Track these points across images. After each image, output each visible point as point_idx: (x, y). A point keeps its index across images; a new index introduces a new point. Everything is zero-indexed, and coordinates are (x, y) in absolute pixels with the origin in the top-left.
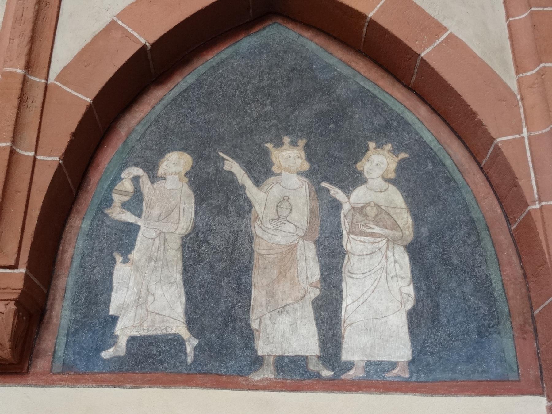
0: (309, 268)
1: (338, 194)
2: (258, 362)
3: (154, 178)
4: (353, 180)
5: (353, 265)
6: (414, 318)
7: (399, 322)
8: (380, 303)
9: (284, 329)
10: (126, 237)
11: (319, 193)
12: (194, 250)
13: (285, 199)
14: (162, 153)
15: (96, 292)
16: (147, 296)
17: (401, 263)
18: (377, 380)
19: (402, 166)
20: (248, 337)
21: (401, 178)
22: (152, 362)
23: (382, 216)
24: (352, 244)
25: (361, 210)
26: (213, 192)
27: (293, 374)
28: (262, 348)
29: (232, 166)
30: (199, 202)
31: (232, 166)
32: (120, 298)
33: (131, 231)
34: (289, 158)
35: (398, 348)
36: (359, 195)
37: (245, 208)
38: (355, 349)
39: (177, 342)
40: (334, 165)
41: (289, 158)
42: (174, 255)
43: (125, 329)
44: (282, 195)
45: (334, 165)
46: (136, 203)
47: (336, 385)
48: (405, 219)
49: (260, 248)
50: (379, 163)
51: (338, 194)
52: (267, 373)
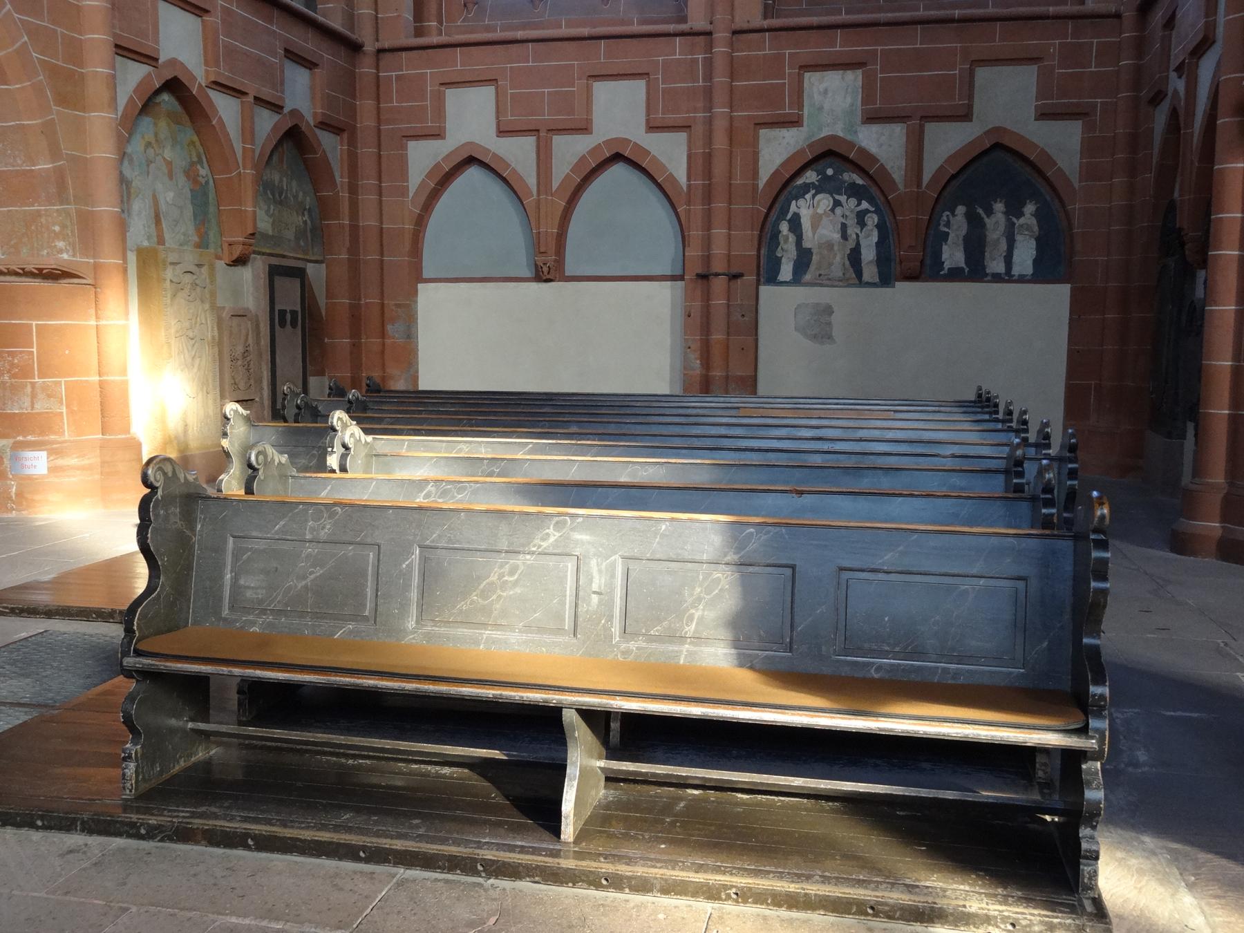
0: (1004, 246)
1: (1014, 220)
2: (987, 275)
3: (954, 215)
4: (1020, 214)
5: (1017, 244)
6: (1035, 261)
7: (1030, 263)
8: (1025, 255)
9: (996, 265)
10: (946, 236)
11: (1008, 220)
13: (997, 222)
14: (955, 207)
15: (937, 254)
16: (953, 255)
18: (1022, 279)
19: (1037, 210)
20: (984, 267)
21: (1037, 214)
22: (955, 275)
23: (1029, 228)
24: (1018, 238)
25: (1021, 226)
26: (975, 223)
27: (997, 278)
28: (988, 271)
29: (980, 211)
30: (969, 223)
31: (980, 211)
32: (945, 256)
33: (948, 234)
34: (999, 207)
35: (1028, 270)
36: (1022, 220)
37: (983, 226)
38: (1016, 271)
39: (962, 269)
40: (1014, 210)
41: (999, 207)
42: (961, 241)
43: (947, 265)
44: (996, 222)
45: (1014, 210)
46: (948, 224)
48: (1036, 229)
49: (988, 239)
50: (1030, 208)
51: (1014, 220)
52: (989, 278)
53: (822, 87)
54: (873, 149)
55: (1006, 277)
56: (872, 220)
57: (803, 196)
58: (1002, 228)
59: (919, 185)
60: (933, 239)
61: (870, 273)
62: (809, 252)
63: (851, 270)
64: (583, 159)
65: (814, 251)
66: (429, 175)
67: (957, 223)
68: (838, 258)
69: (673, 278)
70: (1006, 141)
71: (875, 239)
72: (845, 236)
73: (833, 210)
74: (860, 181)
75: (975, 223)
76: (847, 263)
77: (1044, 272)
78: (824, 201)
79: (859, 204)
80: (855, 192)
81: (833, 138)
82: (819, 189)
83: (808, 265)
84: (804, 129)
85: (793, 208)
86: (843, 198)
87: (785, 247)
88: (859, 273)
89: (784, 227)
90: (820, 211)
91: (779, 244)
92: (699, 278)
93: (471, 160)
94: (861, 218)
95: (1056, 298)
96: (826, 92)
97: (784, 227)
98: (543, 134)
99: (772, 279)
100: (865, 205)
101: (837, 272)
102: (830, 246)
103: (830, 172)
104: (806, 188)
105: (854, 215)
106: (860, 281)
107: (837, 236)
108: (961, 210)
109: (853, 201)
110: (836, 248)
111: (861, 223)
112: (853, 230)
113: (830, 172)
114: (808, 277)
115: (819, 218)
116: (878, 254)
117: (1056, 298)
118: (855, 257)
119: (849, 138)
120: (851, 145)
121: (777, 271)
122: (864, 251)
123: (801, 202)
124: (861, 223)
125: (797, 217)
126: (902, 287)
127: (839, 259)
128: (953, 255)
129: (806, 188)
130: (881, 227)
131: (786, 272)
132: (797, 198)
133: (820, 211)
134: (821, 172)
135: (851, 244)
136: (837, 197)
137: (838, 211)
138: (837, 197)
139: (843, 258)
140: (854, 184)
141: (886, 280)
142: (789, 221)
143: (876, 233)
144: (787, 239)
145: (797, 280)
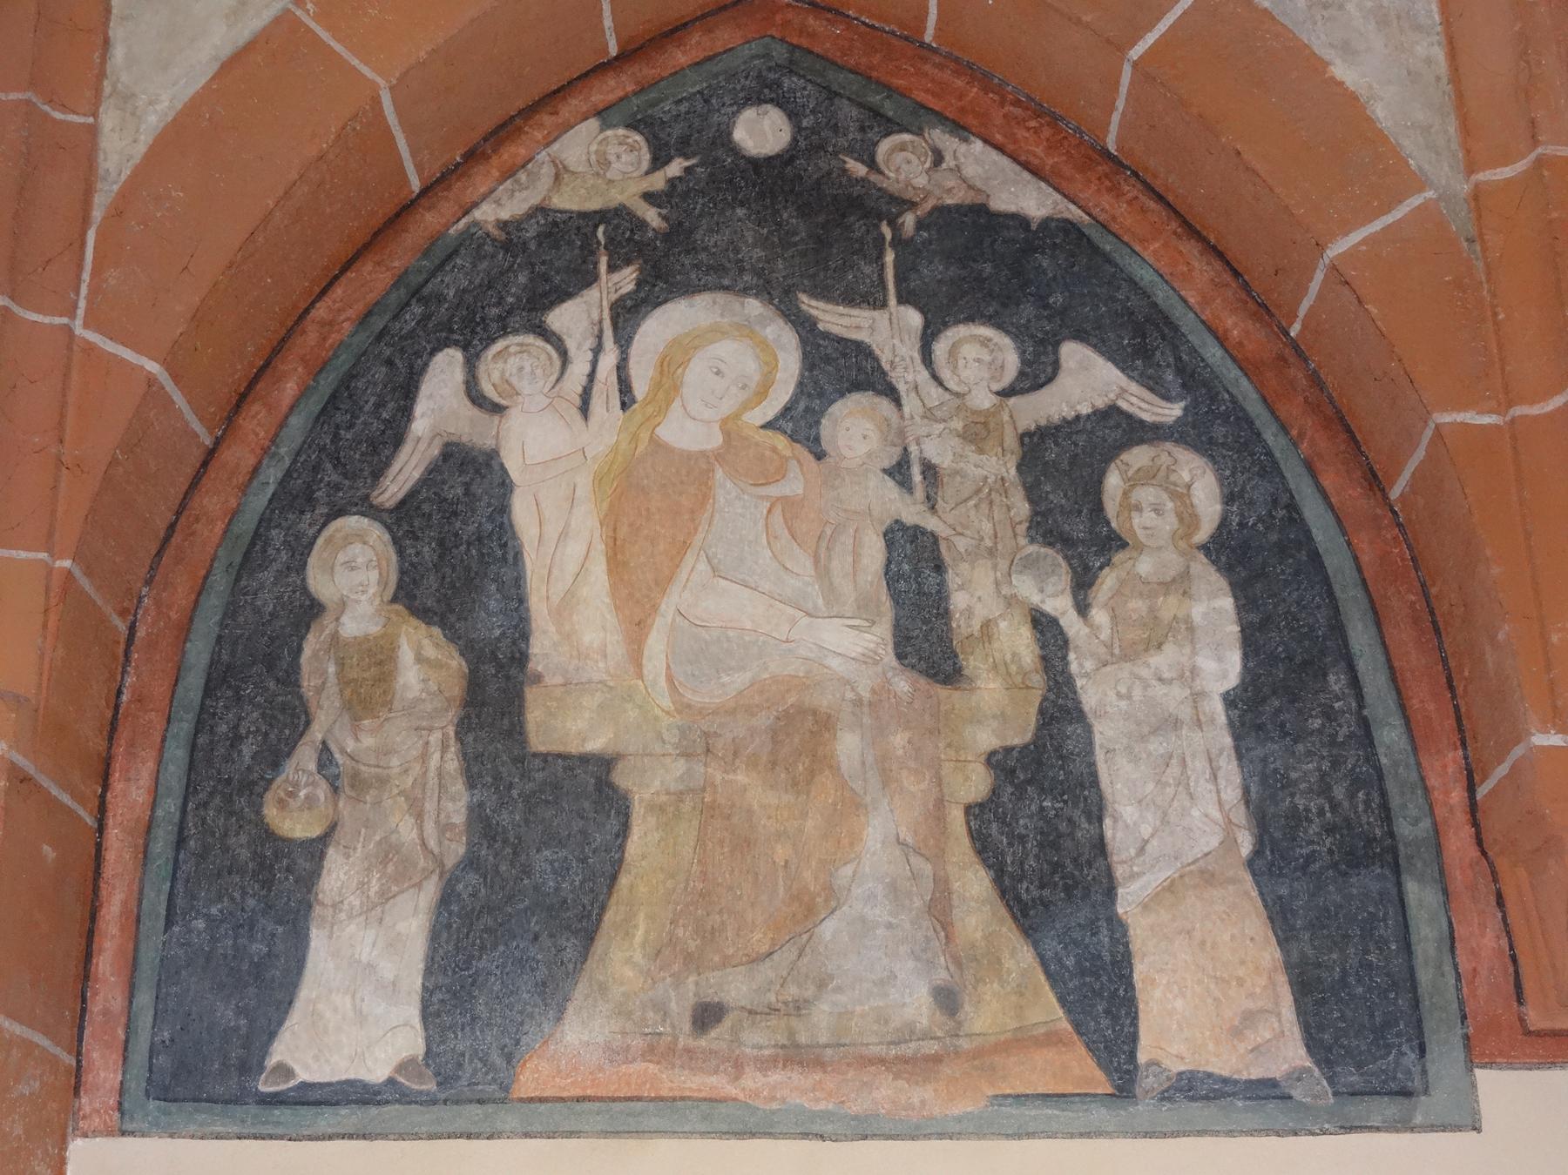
56: (1170, 498)
57: (531, 313)
62: (590, 794)
63: (1020, 958)
65: (645, 786)
71: (1224, 668)
72: (927, 640)
73: (801, 422)
74: (1031, 200)
76: (974, 883)
78: (722, 356)
79: (1037, 372)
82: (667, 261)
85: (439, 403)
86: (889, 331)
87: (357, 744)
88: (1100, 995)
89: (352, 571)
91: (291, 718)
94: (1066, 492)
97: (352, 571)
100: (1088, 379)
105: (1001, 465)
107: (849, 644)
109: (980, 355)
110: (848, 746)
118: (1041, 839)
121: (270, 984)
123: (514, 362)
125: (471, 477)
130: (1262, 556)
131: (358, 997)
132: (473, 330)
133: (687, 430)
135: (995, 710)
136: (835, 319)
137: (854, 426)
138: (835, 319)
139: (931, 846)
142: (403, 520)
143: (1214, 607)
145: (462, 1073)
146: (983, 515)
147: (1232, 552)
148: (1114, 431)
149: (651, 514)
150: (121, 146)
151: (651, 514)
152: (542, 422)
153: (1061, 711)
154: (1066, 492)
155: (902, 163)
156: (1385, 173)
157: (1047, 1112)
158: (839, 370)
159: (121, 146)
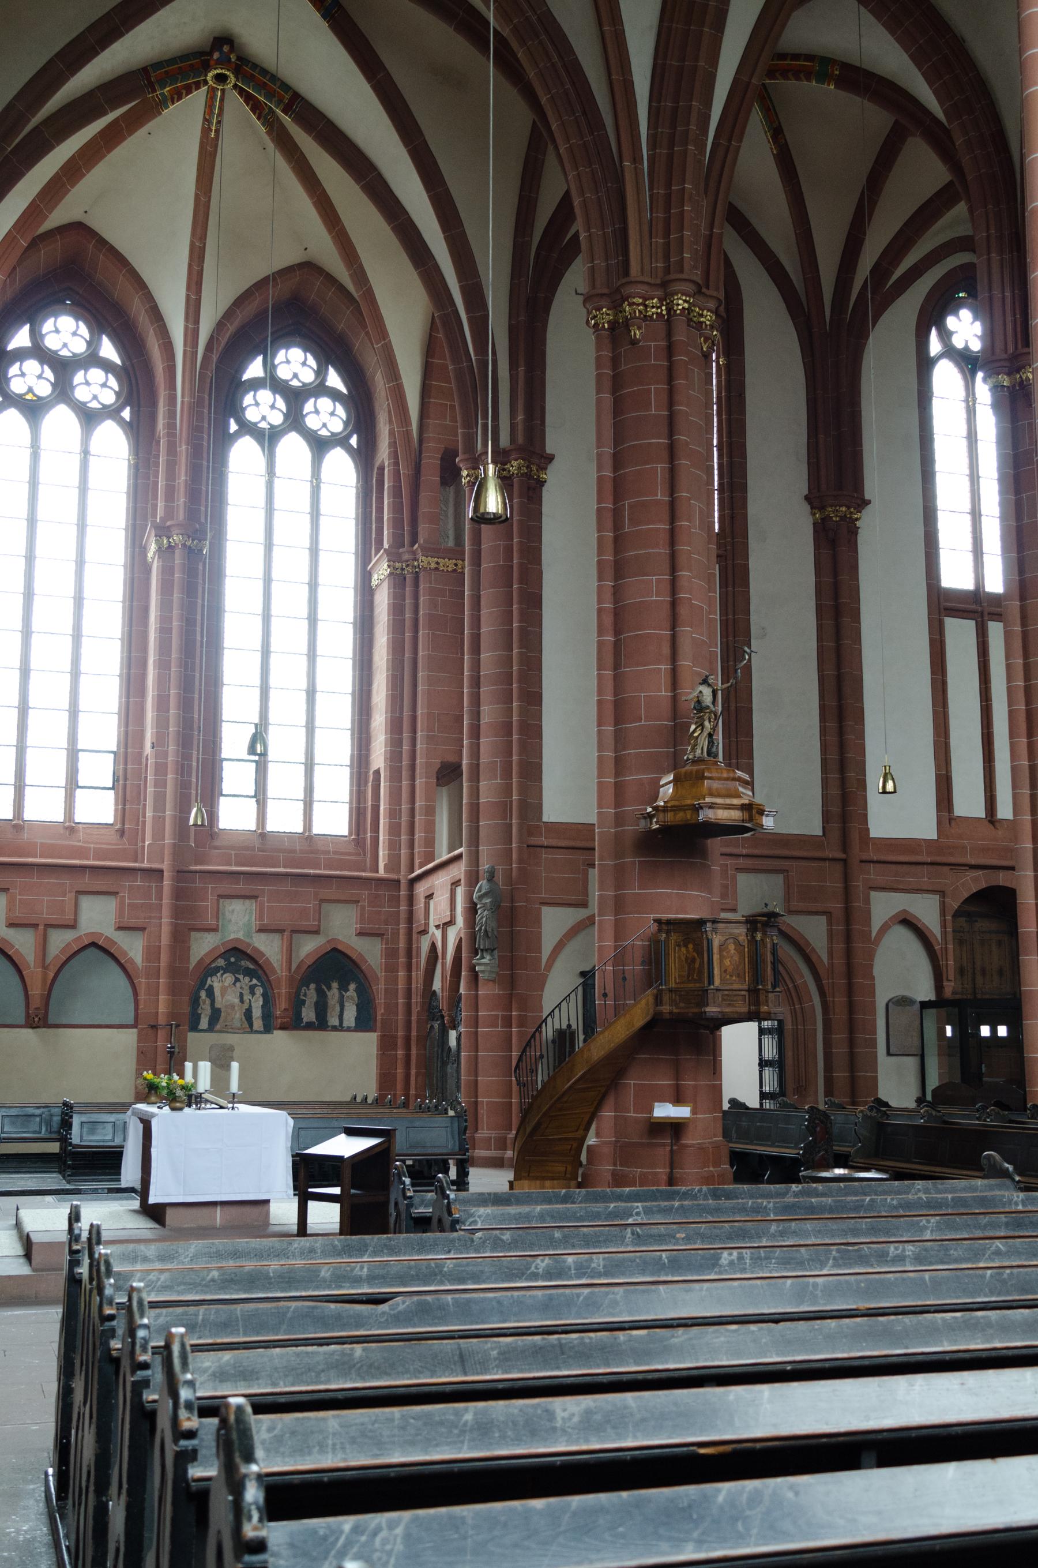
0: (338, 1008)
4: (347, 990)
7: (353, 1019)
8: (350, 1015)
9: (334, 1021)
10: (303, 1002)
11: (340, 993)
12: (317, 1004)
16: (308, 1014)
17: (354, 1008)
18: (349, 1030)
22: (310, 1026)
23: (352, 998)
26: (321, 995)
27: (334, 1029)
29: (324, 987)
31: (324, 987)
32: (304, 1014)
34: (335, 985)
38: (345, 1024)
40: (343, 988)
41: (335, 985)
43: (305, 1020)
44: (333, 994)
45: (343, 988)
46: (305, 995)
47: (342, 1031)
48: (356, 999)
50: (352, 986)
53: (231, 908)
54: (262, 948)
55: (340, 1028)
56: (259, 991)
58: (336, 998)
59: (290, 969)
60: (297, 1004)
61: (258, 1024)
62: (219, 1011)
64: (68, 945)
66: (63, 951)
67: (311, 995)
68: (238, 1016)
69: (134, 1026)
70: (340, 948)
71: (261, 1003)
72: (242, 1001)
73: (234, 984)
74: (252, 967)
75: (321, 995)
77: (364, 1023)
78: (229, 978)
80: (249, 973)
81: (238, 940)
83: (218, 1020)
84: (219, 934)
85: (209, 982)
86: (241, 977)
88: (251, 1025)
90: (226, 984)
92: (145, 1025)
93: (94, 944)
94: (252, 990)
95: (368, 1042)
96: (233, 911)
98: (42, 928)
99: (194, 1027)
100: (255, 981)
101: (237, 1024)
102: (233, 1007)
103: (232, 960)
104: (217, 969)
106: (251, 1030)
107: (237, 1001)
108: (312, 986)
109: (247, 979)
111: (253, 993)
112: (247, 997)
113: (232, 960)
114: (218, 1027)
115: (227, 991)
116: (263, 1012)
117: (368, 1042)
118: (248, 1014)
119: (247, 940)
120: (249, 945)
121: (198, 1023)
122: (254, 1010)
123: (214, 978)
124: (253, 993)
125: (211, 987)
126: (278, 1033)
127: (238, 1015)
128: (308, 1014)
129: (217, 969)
130: (265, 995)
131: (204, 1023)
133: (226, 984)
134: (227, 960)
135: (246, 1006)
137: (238, 984)
140: (247, 968)
141: (268, 1029)
142: (206, 990)
143: (261, 999)
144: (204, 1003)
145: (211, 1029)
146: (246, 992)
147: (263, 995)
148: (256, 985)
149: (224, 990)
150: (191, 968)
151: (224, 990)
152: (217, 983)
153: (250, 1006)
154: (252, 990)
155: (243, 963)
156: (275, 972)
157: (248, 1032)
158: (237, 980)
159: (191, 968)
